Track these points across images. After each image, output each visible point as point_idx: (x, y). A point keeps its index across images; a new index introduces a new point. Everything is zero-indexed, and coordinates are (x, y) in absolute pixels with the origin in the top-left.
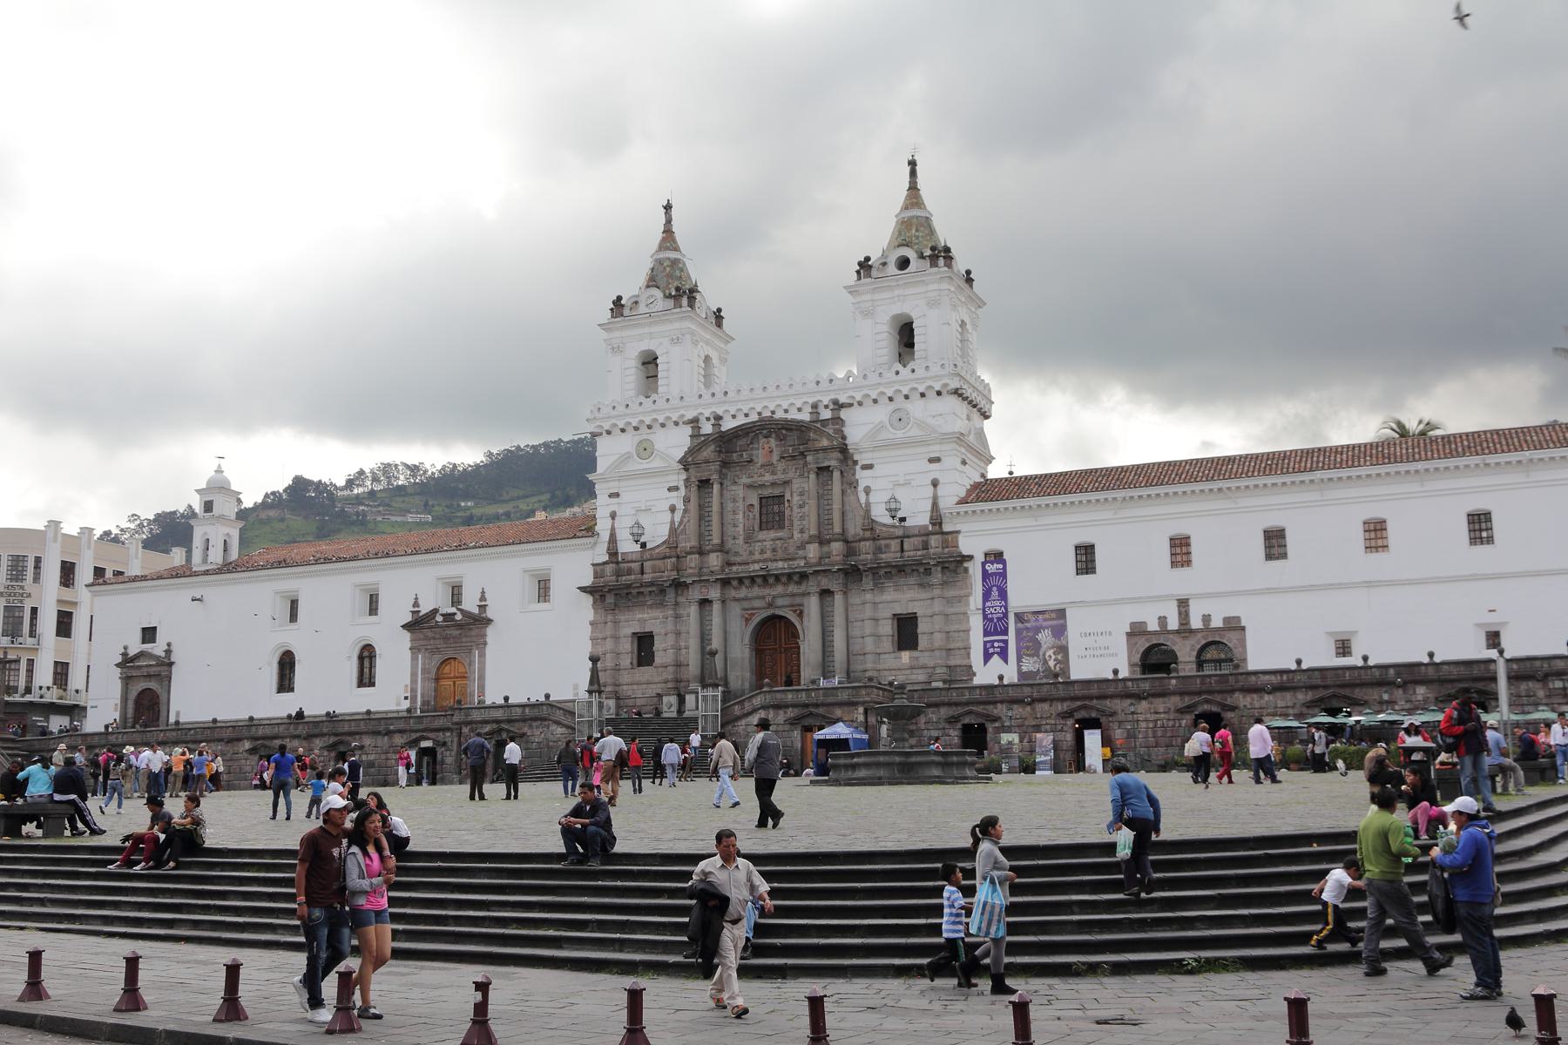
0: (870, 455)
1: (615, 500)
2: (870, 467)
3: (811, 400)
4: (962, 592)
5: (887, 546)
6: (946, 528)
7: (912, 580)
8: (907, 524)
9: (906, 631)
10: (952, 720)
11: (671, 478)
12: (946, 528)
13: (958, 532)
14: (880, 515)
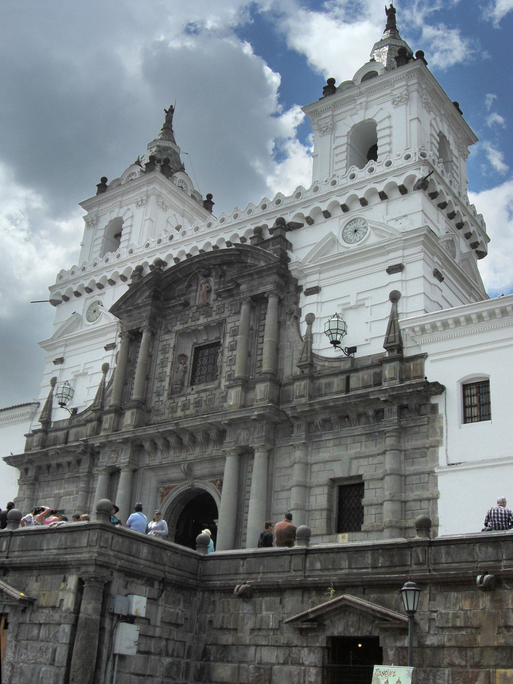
0: (316, 277)
1: (59, 366)
2: (316, 290)
3: (253, 227)
4: (427, 442)
5: (329, 385)
6: (408, 353)
7: (358, 429)
8: (357, 355)
9: (348, 502)
10: (309, 625)
11: (109, 336)
12: (408, 353)
13: (424, 356)
14: (323, 347)
